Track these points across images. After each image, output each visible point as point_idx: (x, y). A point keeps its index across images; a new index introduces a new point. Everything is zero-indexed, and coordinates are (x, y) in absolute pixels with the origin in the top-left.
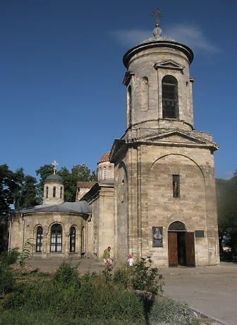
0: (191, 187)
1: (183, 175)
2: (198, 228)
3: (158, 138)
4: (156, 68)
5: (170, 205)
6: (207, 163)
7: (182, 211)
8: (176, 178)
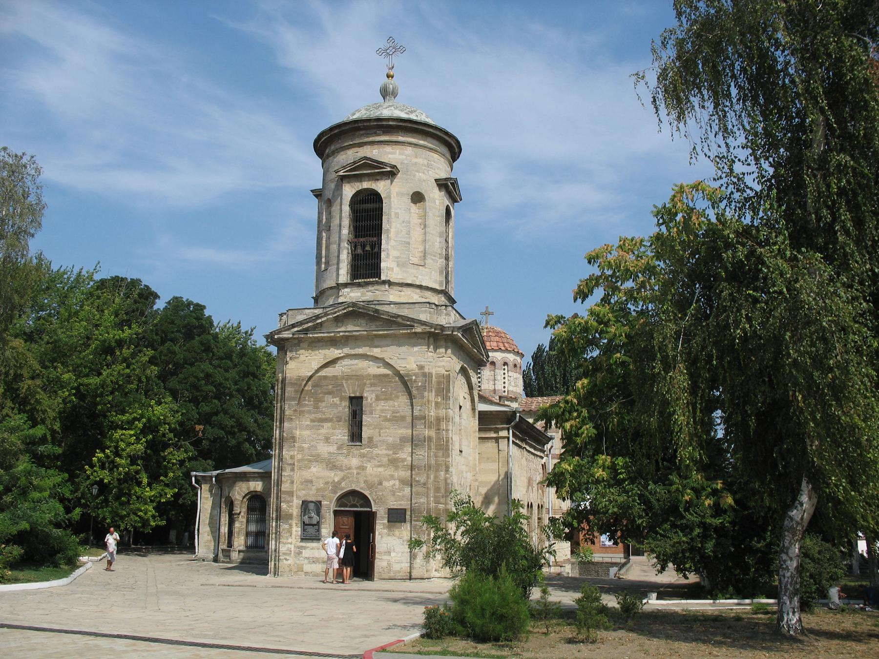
0: (389, 420)
1: (369, 396)
2: (394, 504)
3: (317, 327)
4: (343, 179)
5: (341, 458)
6: (421, 367)
7: (362, 468)
8: (356, 404)
